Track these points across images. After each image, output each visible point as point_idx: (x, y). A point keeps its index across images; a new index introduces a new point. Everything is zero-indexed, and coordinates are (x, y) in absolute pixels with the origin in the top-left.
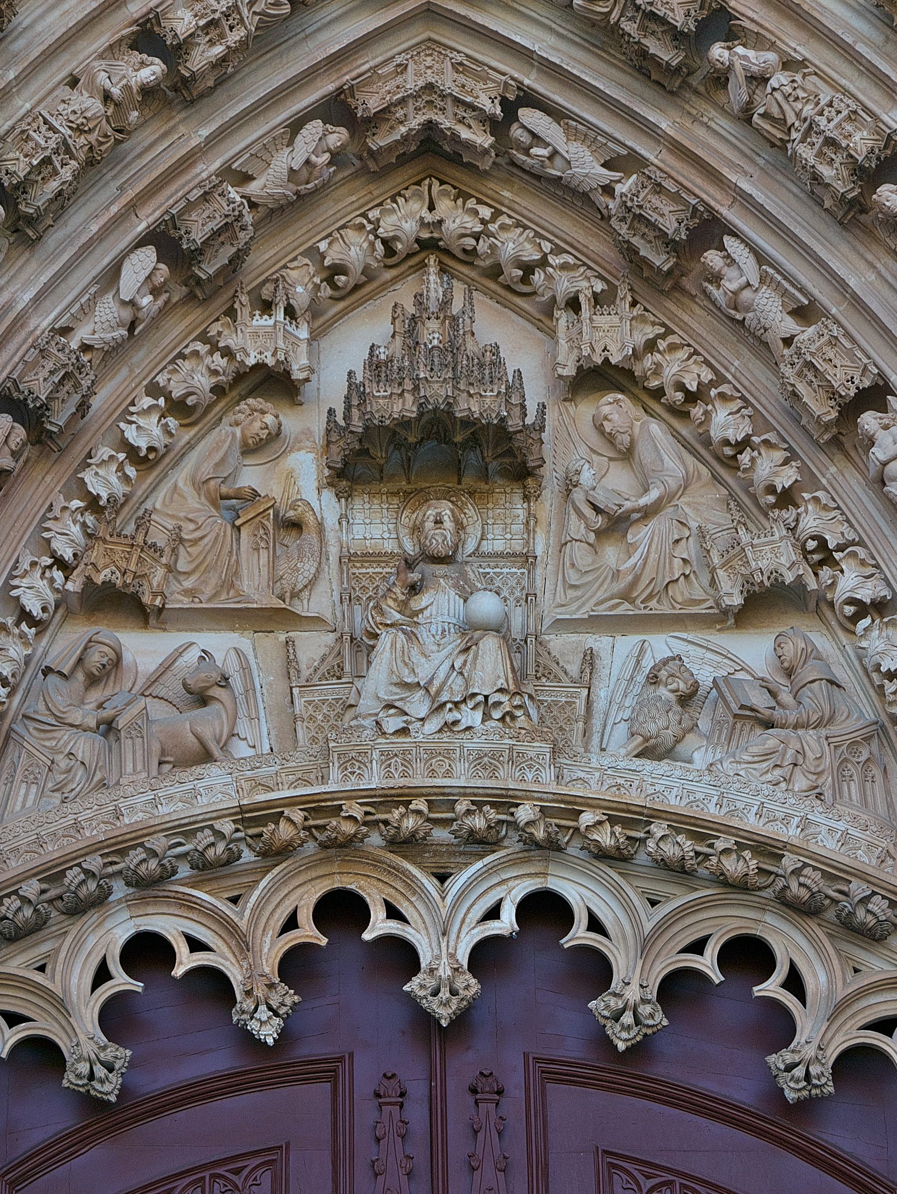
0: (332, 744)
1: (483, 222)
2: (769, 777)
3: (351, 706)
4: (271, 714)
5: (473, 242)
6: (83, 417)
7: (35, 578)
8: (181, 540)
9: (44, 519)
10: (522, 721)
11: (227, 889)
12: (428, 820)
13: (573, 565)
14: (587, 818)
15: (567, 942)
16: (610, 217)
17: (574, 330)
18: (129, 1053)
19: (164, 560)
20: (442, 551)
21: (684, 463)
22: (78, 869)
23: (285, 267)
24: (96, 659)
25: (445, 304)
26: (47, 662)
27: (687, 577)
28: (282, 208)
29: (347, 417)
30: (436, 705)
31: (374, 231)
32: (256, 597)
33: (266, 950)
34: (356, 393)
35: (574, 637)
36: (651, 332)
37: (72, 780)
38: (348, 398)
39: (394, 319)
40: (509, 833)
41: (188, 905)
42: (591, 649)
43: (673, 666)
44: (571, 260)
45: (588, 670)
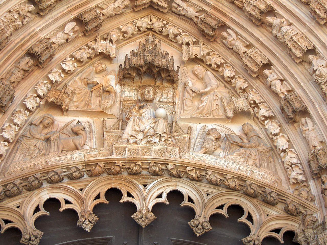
0: (114, 146)
1: (164, 24)
3: (121, 137)
5: (161, 29)
6: (51, 60)
8: (75, 93)
9: (36, 85)
10: (170, 142)
11: (79, 186)
12: (142, 168)
13: (186, 105)
14: (189, 168)
15: (182, 205)
16: (197, 24)
17: (188, 50)
18: (43, 233)
19: (69, 97)
20: (149, 99)
21: (217, 82)
24: (46, 122)
25: (153, 41)
29: (125, 66)
30: (145, 136)
31: (135, 25)
33: (89, 204)
34: (127, 60)
35: (186, 123)
36: (207, 51)
38: (125, 62)
39: (139, 45)
40: (166, 173)
41: (66, 190)
42: (191, 126)
43: (213, 131)
44: (187, 34)
45: (189, 131)
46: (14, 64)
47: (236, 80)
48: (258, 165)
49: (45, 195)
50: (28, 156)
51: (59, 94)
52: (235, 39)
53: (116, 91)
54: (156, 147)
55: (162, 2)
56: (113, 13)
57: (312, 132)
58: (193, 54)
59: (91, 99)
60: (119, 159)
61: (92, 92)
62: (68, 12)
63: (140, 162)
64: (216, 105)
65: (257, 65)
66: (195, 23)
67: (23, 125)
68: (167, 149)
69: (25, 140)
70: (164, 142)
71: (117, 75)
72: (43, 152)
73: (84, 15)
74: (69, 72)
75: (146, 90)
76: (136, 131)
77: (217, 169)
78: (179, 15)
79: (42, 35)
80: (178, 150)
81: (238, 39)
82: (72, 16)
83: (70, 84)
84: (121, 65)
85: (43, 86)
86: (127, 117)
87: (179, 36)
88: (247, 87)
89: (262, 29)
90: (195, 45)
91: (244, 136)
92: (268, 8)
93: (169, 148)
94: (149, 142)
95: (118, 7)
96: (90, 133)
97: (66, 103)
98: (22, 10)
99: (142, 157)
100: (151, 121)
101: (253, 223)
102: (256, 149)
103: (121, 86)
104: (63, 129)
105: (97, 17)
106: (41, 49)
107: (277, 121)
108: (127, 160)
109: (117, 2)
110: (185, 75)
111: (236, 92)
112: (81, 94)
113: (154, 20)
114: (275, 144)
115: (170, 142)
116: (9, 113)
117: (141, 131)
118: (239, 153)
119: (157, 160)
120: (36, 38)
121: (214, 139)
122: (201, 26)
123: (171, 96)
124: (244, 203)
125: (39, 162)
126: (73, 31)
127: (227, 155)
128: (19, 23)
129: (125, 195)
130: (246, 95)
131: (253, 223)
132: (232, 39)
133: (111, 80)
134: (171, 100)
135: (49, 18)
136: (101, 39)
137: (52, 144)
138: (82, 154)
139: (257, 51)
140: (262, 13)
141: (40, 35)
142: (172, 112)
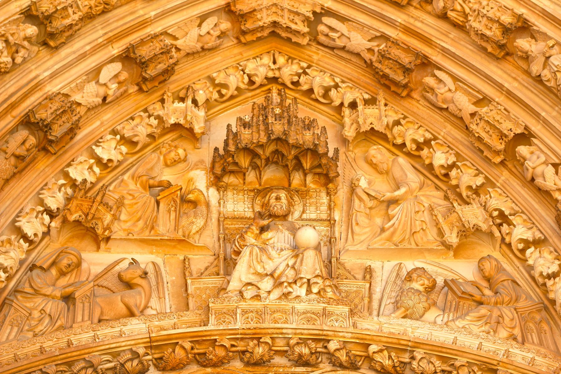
1: (302, 68)
4: (172, 296)
6: (72, 138)
9: (42, 189)
13: (357, 224)
14: (373, 348)
19: (112, 213)
20: (280, 212)
24: (65, 262)
28: (193, 53)
38: (226, 143)
39: (253, 109)
40: (324, 360)
42: (370, 266)
43: (419, 272)
44: (350, 85)
47: (459, 170)
50: (28, 331)
51: (91, 206)
52: (453, 89)
53: (209, 201)
54: (300, 307)
55: (296, 23)
56: (199, 46)
58: (365, 123)
59: (156, 217)
60: (224, 332)
61: (158, 203)
62: (105, 42)
63: (268, 337)
64: (420, 222)
65: (502, 136)
66: (365, 62)
67: (15, 271)
68: (324, 309)
70: (317, 296)
71: (209, 170)
72: (59, 323)
73: (140, 48)
74: (110, 165)
75: (273, 195)
76: (259, 274)
77: (434, 348)
78: (332, 49)
79: (52, 88)
80: (347, 310)
82: (116, 49)
83: (111, 188)
84: (216, 149)
86: (236, 249)
87: (335, 91)
88: (483, 184)
89: (507, 66)
90: (369, 105)
91: (484, 284)
92: (518, 21)
93: (330, 308)
94: (286, 295)
95: (208, 33)
96: (158, 283)
98: (12, 35)
99: (272, 325)
100: (287, 253)
103: (218, 190)
104: (98, 277)
105: (166, 52)
106: (52, 114)
107: (552, 249)
108: (241, 334)
109: (205, 24)
110: (350, 166)
111: (460, 195)
112: (135, 206)
114: (551, 296)
115: (330, 294)
117: (267, 275)
118: (476, 314)
119: (306, 332)
121: (421, 289)
122: (380, 66)
123: (324, 208)
125: (51, 343)
126: (117, 80)
127: (453, 320)
132: (447, 88)
134: (324, 216)
135: (67, 53)
137: (79, 305)
138: (144, 326)
139: (500, 110)
140: (506, 30)
142: (329, 239)
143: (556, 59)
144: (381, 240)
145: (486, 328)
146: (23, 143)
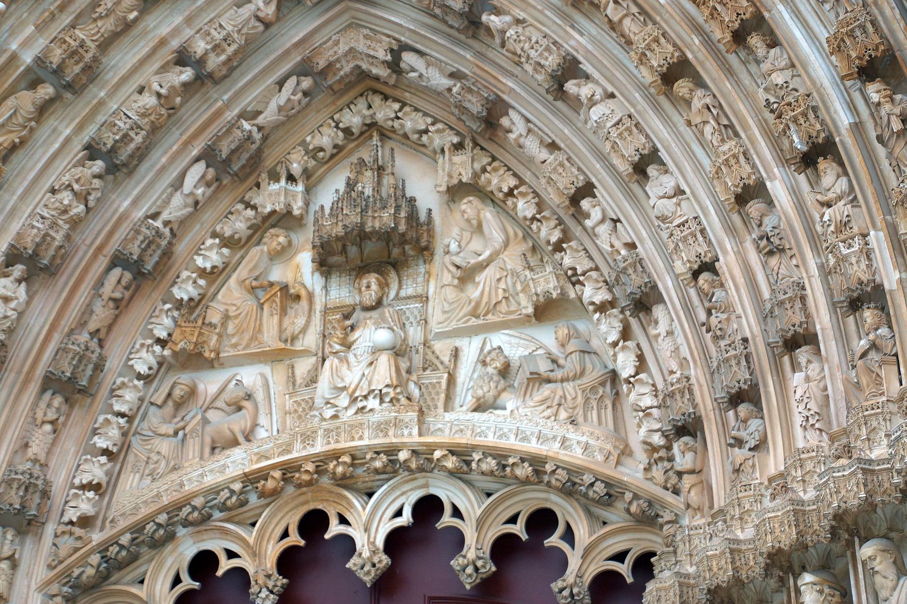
2: (543, 415)
7: (144, 354)
14: (437, 454)
19: (217, 330)
22: (152, 523)
23: (289, 153)
24: (178, 393)
26: (152, 400)
27: (506, 298)
32: (270, 343)
33: (269, 553)
37: (158, 468)
41: (225, 532)
46: (93, 292)
48: (580, 419)
49: (187, 548)
54: (375, 418)
57: (668, 339)
59: (261, 325)
69: (140, 442)
72: (172, 463)
79: (139, 214)
81: (529, 131)
85: (165, 317)
93: (402, 416)
95: (289, 100)
97: (212, 344)
98: (77, 181)
101: (572, 545)
102: (579, 382)
106: (139, 246)
109: (284, 89)
113: (377, 100)
116: (104, 392)
120: (128, 221)
124: (556, 504)
125: (166, 487)
128: (79, 209)
129: (334, 522)
130: (558, 256)
131: (572, 545)
133: (302, 267)
134: (420, 290)
136: (270, 179)
141: (133, 215)
143: (595, 113)
144: (465, 316)
145: (548, 412)
146: (119, 282)
